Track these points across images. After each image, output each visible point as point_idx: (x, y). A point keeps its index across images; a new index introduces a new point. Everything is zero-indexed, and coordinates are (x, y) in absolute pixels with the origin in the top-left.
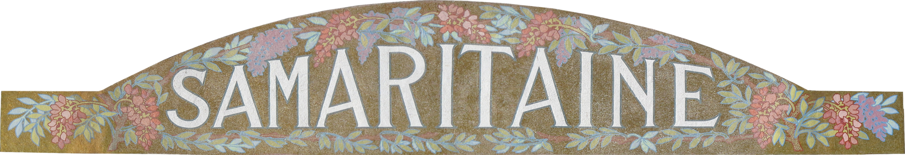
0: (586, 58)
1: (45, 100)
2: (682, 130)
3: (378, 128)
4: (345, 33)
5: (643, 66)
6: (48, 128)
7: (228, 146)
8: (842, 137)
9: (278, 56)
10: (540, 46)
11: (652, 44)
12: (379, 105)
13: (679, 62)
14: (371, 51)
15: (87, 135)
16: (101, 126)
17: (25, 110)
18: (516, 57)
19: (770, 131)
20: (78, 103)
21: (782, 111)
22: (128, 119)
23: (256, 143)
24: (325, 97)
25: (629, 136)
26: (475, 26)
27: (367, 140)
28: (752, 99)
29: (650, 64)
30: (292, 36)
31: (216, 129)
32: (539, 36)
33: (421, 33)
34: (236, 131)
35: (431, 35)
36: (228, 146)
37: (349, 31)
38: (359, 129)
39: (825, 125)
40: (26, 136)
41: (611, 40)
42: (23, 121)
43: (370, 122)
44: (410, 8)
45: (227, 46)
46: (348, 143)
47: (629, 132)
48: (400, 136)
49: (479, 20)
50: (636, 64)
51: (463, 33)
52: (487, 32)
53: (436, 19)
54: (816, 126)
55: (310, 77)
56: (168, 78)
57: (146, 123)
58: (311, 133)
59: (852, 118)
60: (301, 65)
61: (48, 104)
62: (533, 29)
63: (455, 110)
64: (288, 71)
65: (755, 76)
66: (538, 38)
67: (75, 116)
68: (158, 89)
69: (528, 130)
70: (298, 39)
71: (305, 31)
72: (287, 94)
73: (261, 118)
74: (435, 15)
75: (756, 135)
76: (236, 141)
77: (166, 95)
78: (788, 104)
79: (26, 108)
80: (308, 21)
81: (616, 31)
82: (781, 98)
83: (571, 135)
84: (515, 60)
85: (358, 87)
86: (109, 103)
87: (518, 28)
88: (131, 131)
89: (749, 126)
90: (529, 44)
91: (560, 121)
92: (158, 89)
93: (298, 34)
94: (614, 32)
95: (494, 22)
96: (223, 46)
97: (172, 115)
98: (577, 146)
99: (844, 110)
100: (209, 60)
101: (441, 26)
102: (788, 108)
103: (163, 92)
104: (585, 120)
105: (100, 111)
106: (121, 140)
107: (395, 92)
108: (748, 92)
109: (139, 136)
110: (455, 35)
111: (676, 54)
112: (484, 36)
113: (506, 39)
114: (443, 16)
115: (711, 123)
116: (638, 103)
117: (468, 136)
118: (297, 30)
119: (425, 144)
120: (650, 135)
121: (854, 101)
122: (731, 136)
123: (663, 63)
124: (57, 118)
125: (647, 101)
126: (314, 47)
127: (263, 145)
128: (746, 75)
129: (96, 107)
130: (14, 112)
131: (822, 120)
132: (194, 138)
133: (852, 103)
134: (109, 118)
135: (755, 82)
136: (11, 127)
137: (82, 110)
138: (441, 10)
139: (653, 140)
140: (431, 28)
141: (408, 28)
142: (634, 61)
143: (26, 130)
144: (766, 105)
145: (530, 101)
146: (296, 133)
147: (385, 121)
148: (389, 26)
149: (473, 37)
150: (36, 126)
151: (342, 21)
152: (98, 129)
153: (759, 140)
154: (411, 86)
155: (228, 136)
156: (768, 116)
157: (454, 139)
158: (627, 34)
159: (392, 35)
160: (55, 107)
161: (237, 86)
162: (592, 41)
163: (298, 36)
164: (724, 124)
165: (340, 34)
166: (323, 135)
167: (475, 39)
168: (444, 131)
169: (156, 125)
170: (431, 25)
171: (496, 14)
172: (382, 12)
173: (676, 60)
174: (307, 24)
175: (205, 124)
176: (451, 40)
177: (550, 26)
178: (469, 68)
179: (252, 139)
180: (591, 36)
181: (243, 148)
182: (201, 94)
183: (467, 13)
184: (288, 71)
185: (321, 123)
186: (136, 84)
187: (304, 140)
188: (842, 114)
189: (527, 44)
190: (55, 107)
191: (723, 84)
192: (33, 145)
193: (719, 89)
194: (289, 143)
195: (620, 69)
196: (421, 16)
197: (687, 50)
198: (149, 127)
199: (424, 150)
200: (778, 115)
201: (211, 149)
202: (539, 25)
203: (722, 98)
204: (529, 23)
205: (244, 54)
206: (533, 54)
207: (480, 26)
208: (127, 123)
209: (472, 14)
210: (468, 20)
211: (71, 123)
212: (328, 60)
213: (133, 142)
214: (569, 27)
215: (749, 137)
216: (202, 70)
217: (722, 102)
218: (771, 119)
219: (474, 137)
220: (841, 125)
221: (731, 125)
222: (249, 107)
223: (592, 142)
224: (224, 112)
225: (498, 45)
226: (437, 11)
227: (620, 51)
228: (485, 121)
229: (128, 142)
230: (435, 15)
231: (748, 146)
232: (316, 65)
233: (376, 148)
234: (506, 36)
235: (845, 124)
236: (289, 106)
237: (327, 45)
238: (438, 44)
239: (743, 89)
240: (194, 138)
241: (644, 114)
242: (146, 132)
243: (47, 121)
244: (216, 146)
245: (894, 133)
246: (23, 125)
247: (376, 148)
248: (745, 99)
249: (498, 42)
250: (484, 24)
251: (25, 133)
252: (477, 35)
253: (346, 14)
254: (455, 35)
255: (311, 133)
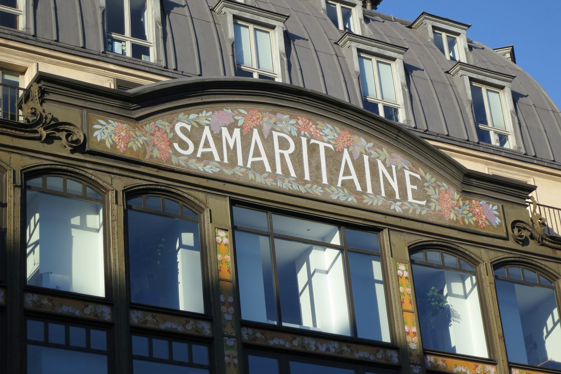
0: (366, 158)
1: (111, 124)
2: (412, 204)
3: (276, 174)
4: (256, 121)
5: (391, 167)
6: (114, 140)
7: (204, 168)
8: (478, 222)
9: (225, 125)
10: (345, 147)
11: (393, 157)
12: (275, 162)
13: (405, 169)
14: (269, 133)
15: (135, 148)
16: (141, 144)
17: (102, 127)
18: (335, 150)
19: (449, 212)
20: (128, 129)
21: (452, 203)
22: (154, 143)
23: (218, 170)
24: (249, 152)
25: (390, 202)
26: (315, 131)
27: (271, 179)
28: (439, 194)
29: (394, 167)
30: (231, 117)
31: (198, 158)
32: (344, 142)
33: (291, 129)
34: (208, 161)
35: (296, 130)
36: (204, 168)
37: (258, 120)
38: (267, 172)
39: (470, 215)
40: (103, 142)
41: (375, 152)
42: (101, 133)
43: (272, 170)
44: (285, 115)
45: (200, 115)
46: (263, 179)
47: (389, 200)
48: (287, 181)
49: (316, 128)
50: (388, 166)
51: (310, 133)
52: (321, 135)
53: (297, 123)
54: (468, 214)
55: (241, 140)
56: (172, 124)
57: (163, 147)
58: (244, 170)
59: (482, 213)
60: (237, 132)
61: (113, 126)
62: (341, 138)
63: (311, 172)
64: (231, 134)
65: (439, 183)
66: (344, 143)
67: (127, 135)
68: (168, 131)
69: (345, 189)
70: (234, 119)
71: (237, 115)
72: (232, 147)
73: (220, 157)
74: (297, 121)
75: (444, 213)
76: (208, 167)
77: (172, 134)
78: (454, 200)
79: (102, 126)
80: (238, 110)
81: (377, 147)
82: (451, 197)
83: (364, 196)
84: (335, 152)
85: (265, 150)
86: (144, 133)
87: (334, 136)
88: (156, 150)
89: (440, 208)
90: (340, 145)
91: (359, 188)
92: (168, 131)
93: (234, 116)
94: (376, 148)
95: (323, 131)
96: (199, 114)
97: (176, 145)
98: (367, 203)
99: (477, 208)
100: (192, 120)
101: (300, 127)
102: (455, 202)
103: (170, 132)
104: (370, 190)
105: (140, 136)
106: (151, 154)
107: (282, 156)
108: (437, 191)
109: (160, 154)
110: (306, 133)
111: (404, 165)
112: (320, 137)
113: (329, 140)
114: (300, 122)
115: (424, 203)
116: (391, 186)
117: (318, 187)
118: (233, 114)
119: (298, 187)
120: (399, 203)
121: (481, 205)
122: (433, 211)
123: (399, 168)
124: (118, 135)
125: (395, 185)
126: (242, 125)
127: (221, 171)
128: (435, 182)
129: (138, 133)
130: (96, 126)
131: (470, 212)
132: (187, 161)
133: (480, 205)
134: (145, 140)
135: (439, 186)
136: (95, 135)
137: (131, 133)
138: (299, 119)
139: (400, 206)
140: (295, 127)
141: (285, 124)
142: (387, 164)
143: (103, 138)
144: (445, 199)
145: (344, 175)
146: (237, 168)
147: (279, 171)
148: (276, 122)
149: (315, 136)
150: (108, 137)
151: (254, 114)
152: (140, 146)
153: (445, 216)
154: (289, 154)
155: (204, 163)
156: (447, 205)
157: (311, 188)
158: (382, 150)
159: (278, 127)
160: (116, 128)
161: (206, 136)
162: (368, 150)
163: (234, 117)
164: (429, 204)
165: (254, 121)
166: (250, 172)
167: (316, 137)
168: (306, 182)
169: (168, 149)
170: (295, 125)
171: (324, 127)
172: (272, 114)
173: (404, 168)
174: (238, 112)
175: (192, 154)
176: (305, 136)
177: (349, 138)
178: (314, 152)
179: (216, 167)
180: (367, 147)
181: (212, 171)
182: (189, 137)
183: (311, 124)
184: (231, 134)
185: (249, 166)
186: (157, 125)
187: (241, 173)
188: (477, 210)
189: (339, 145)
190: (116, 128)
191: (426, 184)
192: (107, 148)
193: (424, 187)
194: (234, 173)
195: (381, 167)
196: (290, 120)
197: (408, 164)
198: (165, 150)
199: (298, 190)
200: (451, 205)
201: (196, 168)
202: (343, 137)
203: (427, 191)
204: (339, 135)
205: (209, 121)
206: (343, 150)
207: (317, 131)
208: (154, 145)
209: (313, 124)
210: (312, 127)
211: (126, 139)
212: (250, 133)
213: (158, 156)
214: (356, 141)
215: (441, 213)
216: (189, 125)
217: (427, 193)
218: (449, 207)
219: (321, 188)
220: (477, 215)
221: (432, 205)
222: (213, 149)
223: (374, 202)
224: (201, 150)
225: (326, 143)
226: (297, 119)
227: (380, 158)
228: (325, 181)
229: (155, 156)
230: (297, 121)
231: (441, 218)
232: (244, 134)
233: (276, 184)
234: (329, 139)
235: (479, 215)
236: (233, 153)
237: (248, 125)
238: (299, 136)
239: (435, 189)
240: (187, 161)
241: (394, 192)
242: (164, 152)
243: (113, 136)
244: (198, 167)
245: (499, 224)
246: (101, 135)
247: (276, 184)
248: (436, 194)
249: (326, 141)
250: (319, 131)
251: (102, 140)
252: (316, 135)
253: (256, 111)
254: (306, 133)
255: (243, 170)
